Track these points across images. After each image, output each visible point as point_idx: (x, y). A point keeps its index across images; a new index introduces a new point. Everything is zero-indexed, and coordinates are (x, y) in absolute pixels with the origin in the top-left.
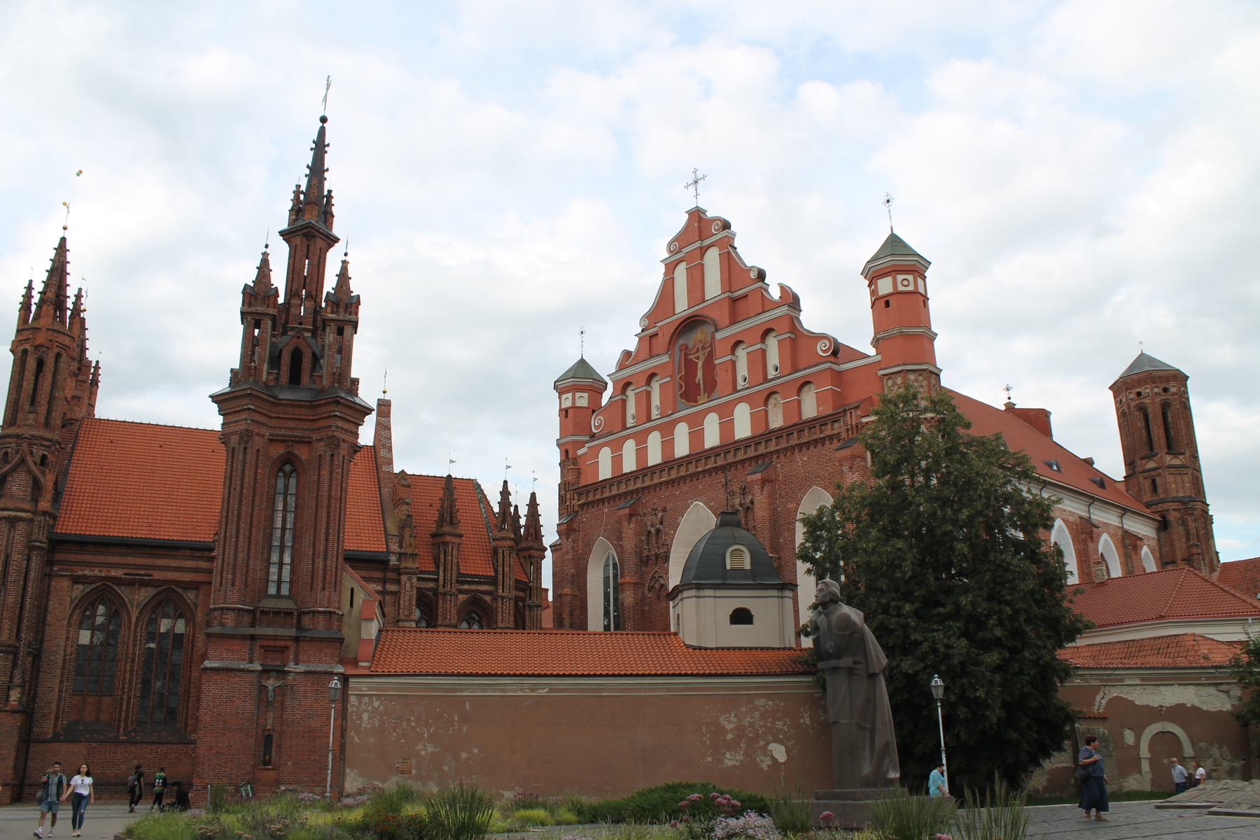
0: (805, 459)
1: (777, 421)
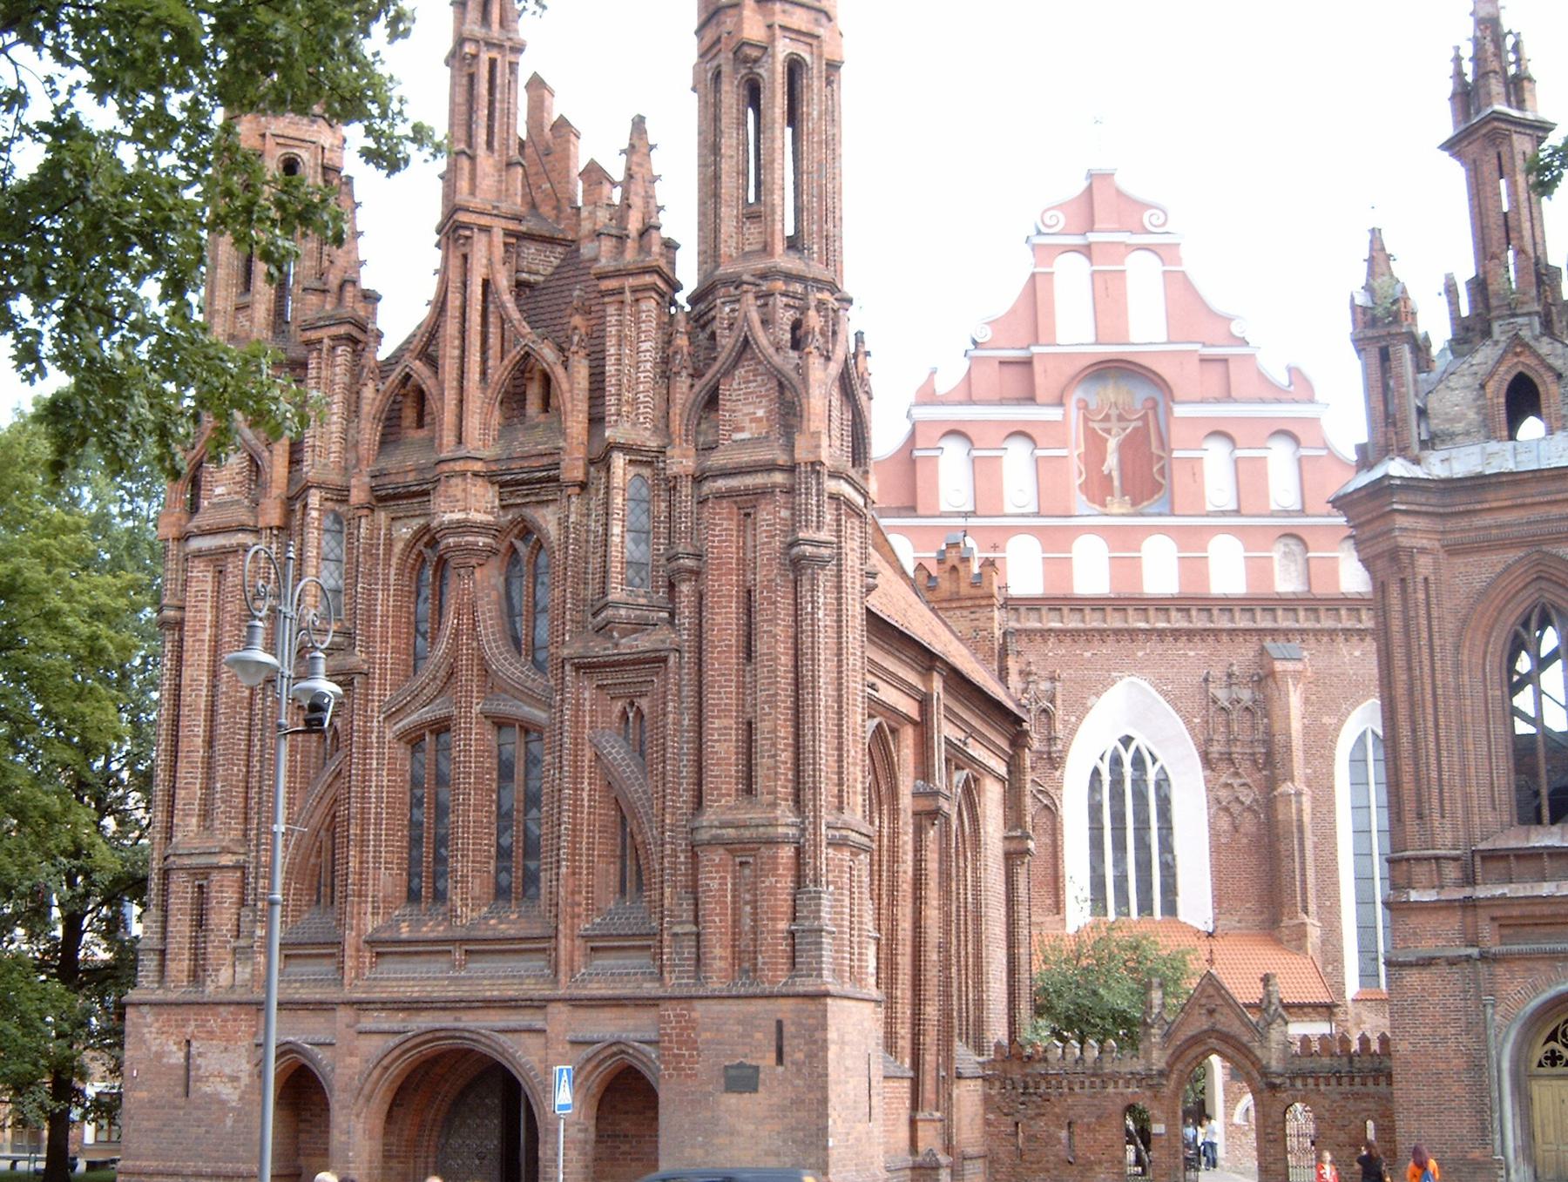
0: (1357, 653)
1: (1287, 582)
